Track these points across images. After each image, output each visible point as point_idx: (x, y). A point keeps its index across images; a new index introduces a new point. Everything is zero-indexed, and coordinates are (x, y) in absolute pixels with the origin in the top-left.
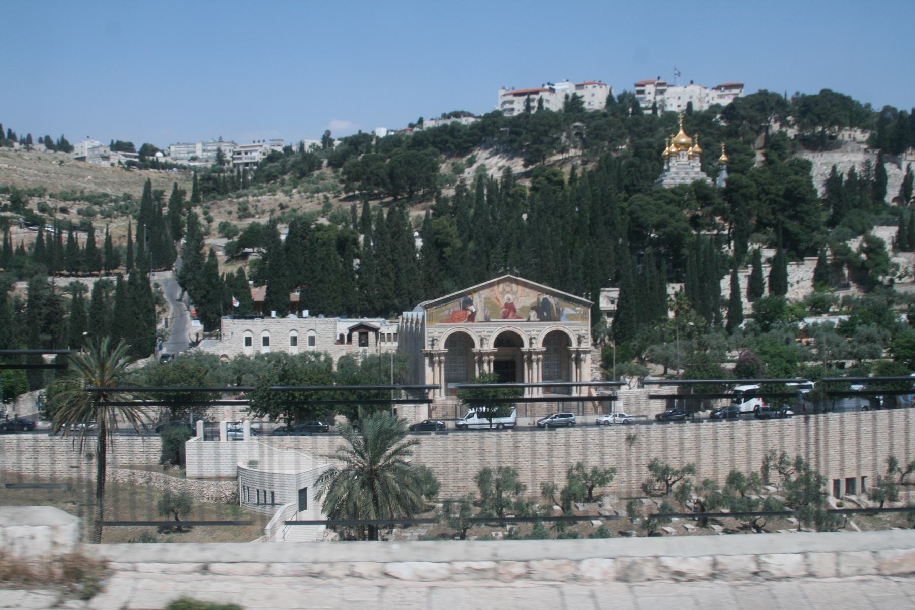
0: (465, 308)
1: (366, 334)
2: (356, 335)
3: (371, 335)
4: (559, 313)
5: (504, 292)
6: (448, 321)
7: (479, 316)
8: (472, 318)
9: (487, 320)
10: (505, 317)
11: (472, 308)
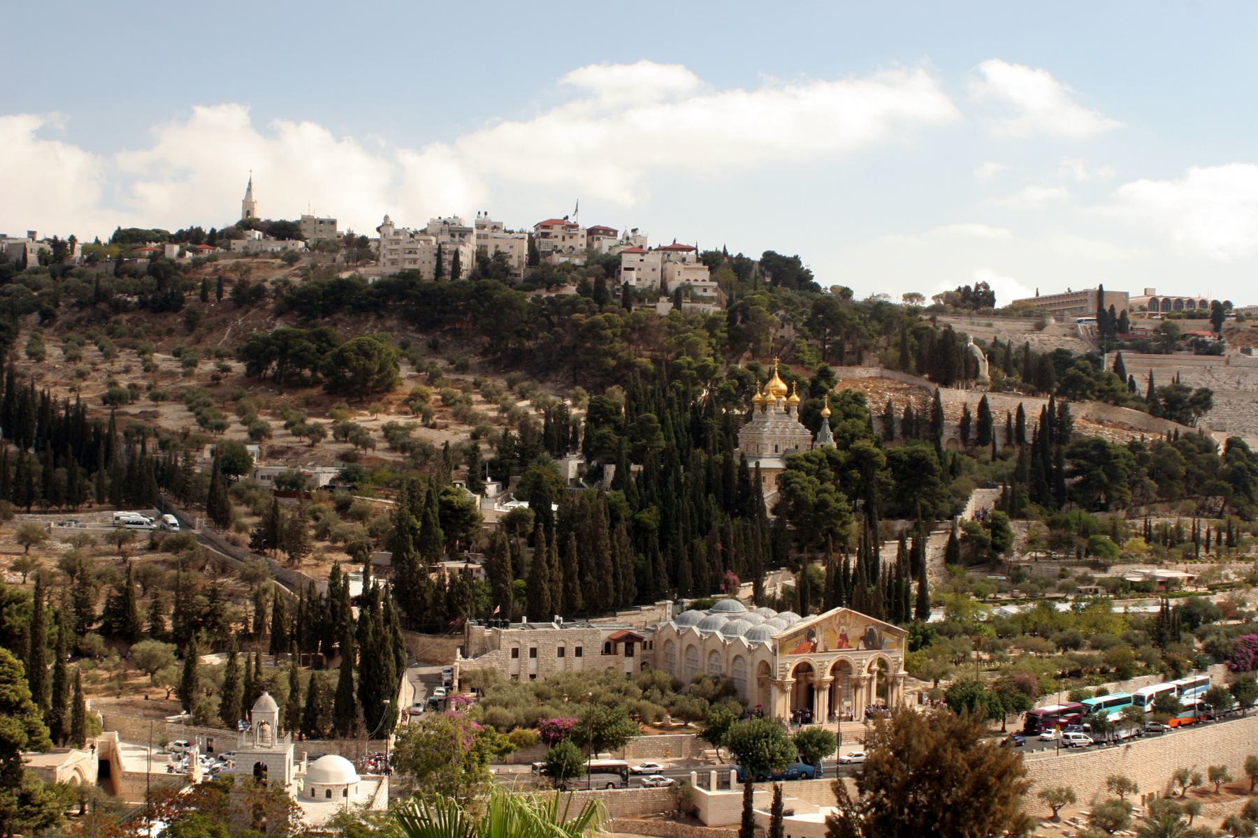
0: (809, 640)
1: (632, 644)
2: (621, 647)
3: (637, 645)
4: (881, 641)
5: (840, 624)
6: (795, 652)
7: (820, 648)
8: (814, 649)
9: (826, 650)
10: (840, 647)
11: (814, 639)
